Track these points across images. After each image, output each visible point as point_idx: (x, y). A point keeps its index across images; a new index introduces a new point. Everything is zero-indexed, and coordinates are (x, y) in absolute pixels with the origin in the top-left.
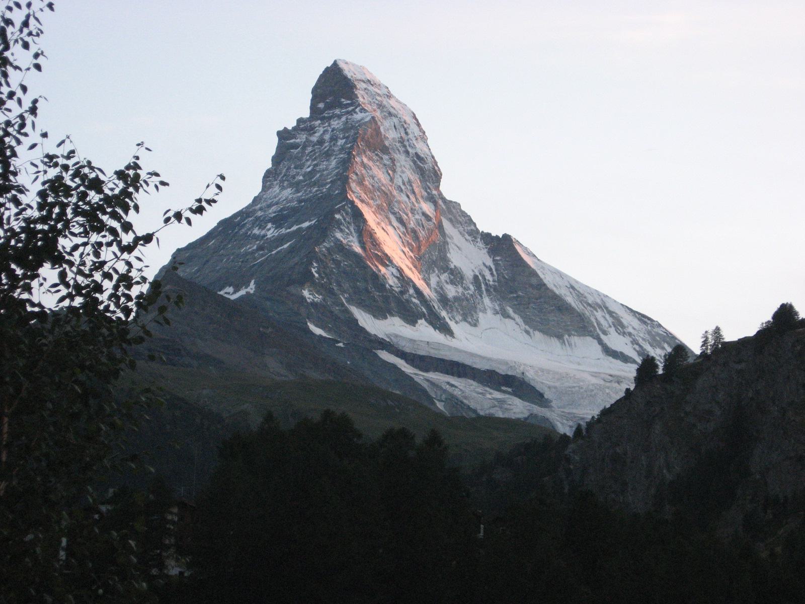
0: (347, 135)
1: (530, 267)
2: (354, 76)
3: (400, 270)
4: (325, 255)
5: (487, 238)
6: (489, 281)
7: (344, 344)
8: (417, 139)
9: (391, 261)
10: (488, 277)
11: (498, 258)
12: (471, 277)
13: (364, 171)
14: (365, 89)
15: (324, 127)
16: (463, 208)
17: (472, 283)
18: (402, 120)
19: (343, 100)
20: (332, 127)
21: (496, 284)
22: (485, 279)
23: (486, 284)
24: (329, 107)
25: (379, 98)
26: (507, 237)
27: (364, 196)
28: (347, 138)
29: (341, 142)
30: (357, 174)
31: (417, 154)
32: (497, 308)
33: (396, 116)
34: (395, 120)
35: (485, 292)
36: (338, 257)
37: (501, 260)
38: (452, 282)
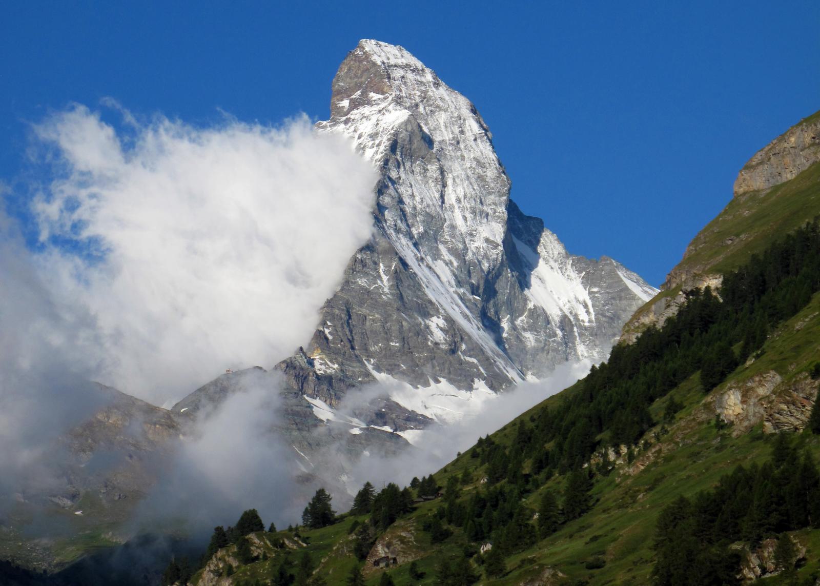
0: (377, 142)
2: (385, 61)
3: (449, 320)
4: (343, 310)
6: (583, 321)
7: (361, 429)
11: (595, 290)
12: (557, 319)
14: (403, 77)
15: (349, 133)
17: (559, 327)
19: (372, 94)
20: (359, 132)
21: (594, 325)
24: (355, 105)
25: (423, 88)
28: (379, 145)
29: (369, 153)
33: (446, 111)
35: (578, 338)
37: (598, 292)
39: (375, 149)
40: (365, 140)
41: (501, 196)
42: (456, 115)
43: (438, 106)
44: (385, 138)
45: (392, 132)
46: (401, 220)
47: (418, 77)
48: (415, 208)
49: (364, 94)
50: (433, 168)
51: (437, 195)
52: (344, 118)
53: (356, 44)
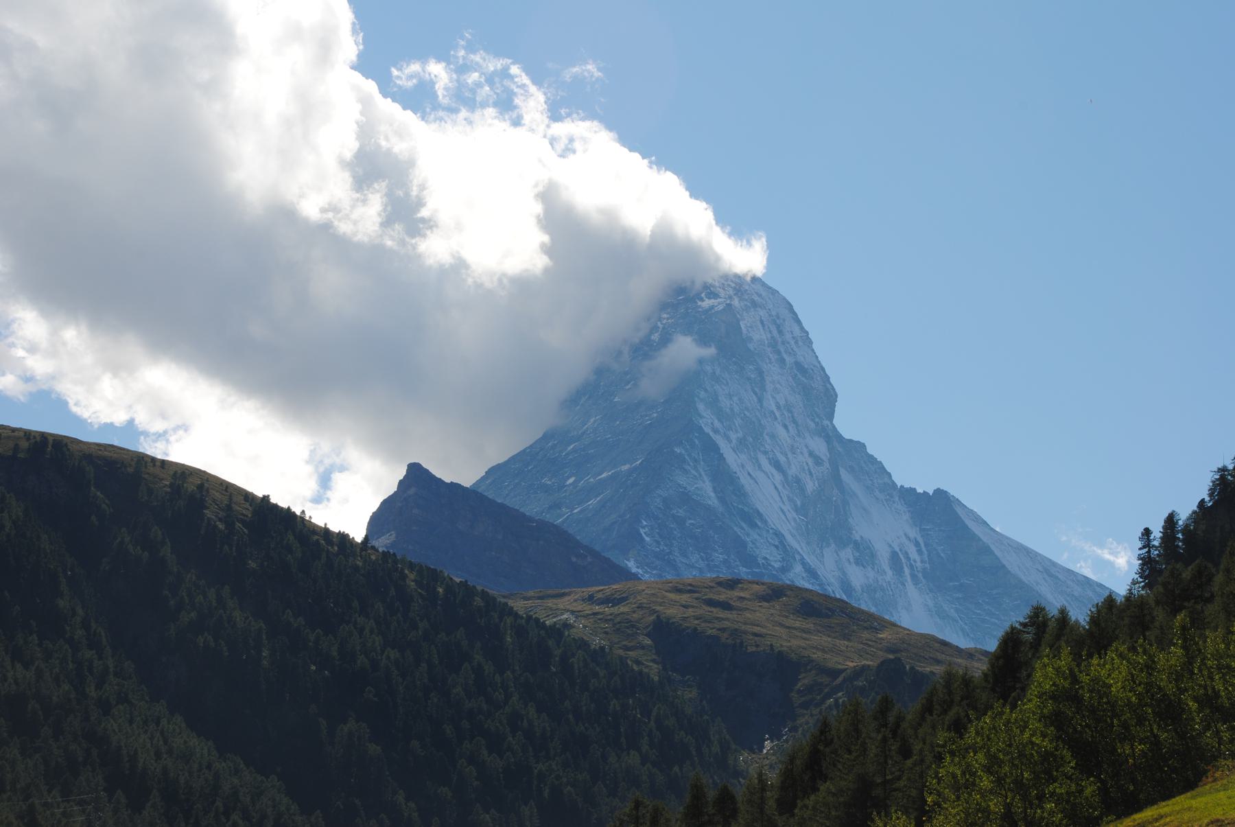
1: (980, 539)
3: (778, 534)
5: (909, 495)
8: (796, 343)
9: (765, 522)
10: (914, 555)
13: (717, 387)
16: (870, 451)
18: (774, 313)
22: (908, 558)
23: (911, 567)
26: (939, 492)
27: (717, 424)
30: (706, 390)
31: (798, 365)
32: (931, 603)
34: (762, 313)
36: (681, 513)
38: (858, 562)
48: (732, 410)
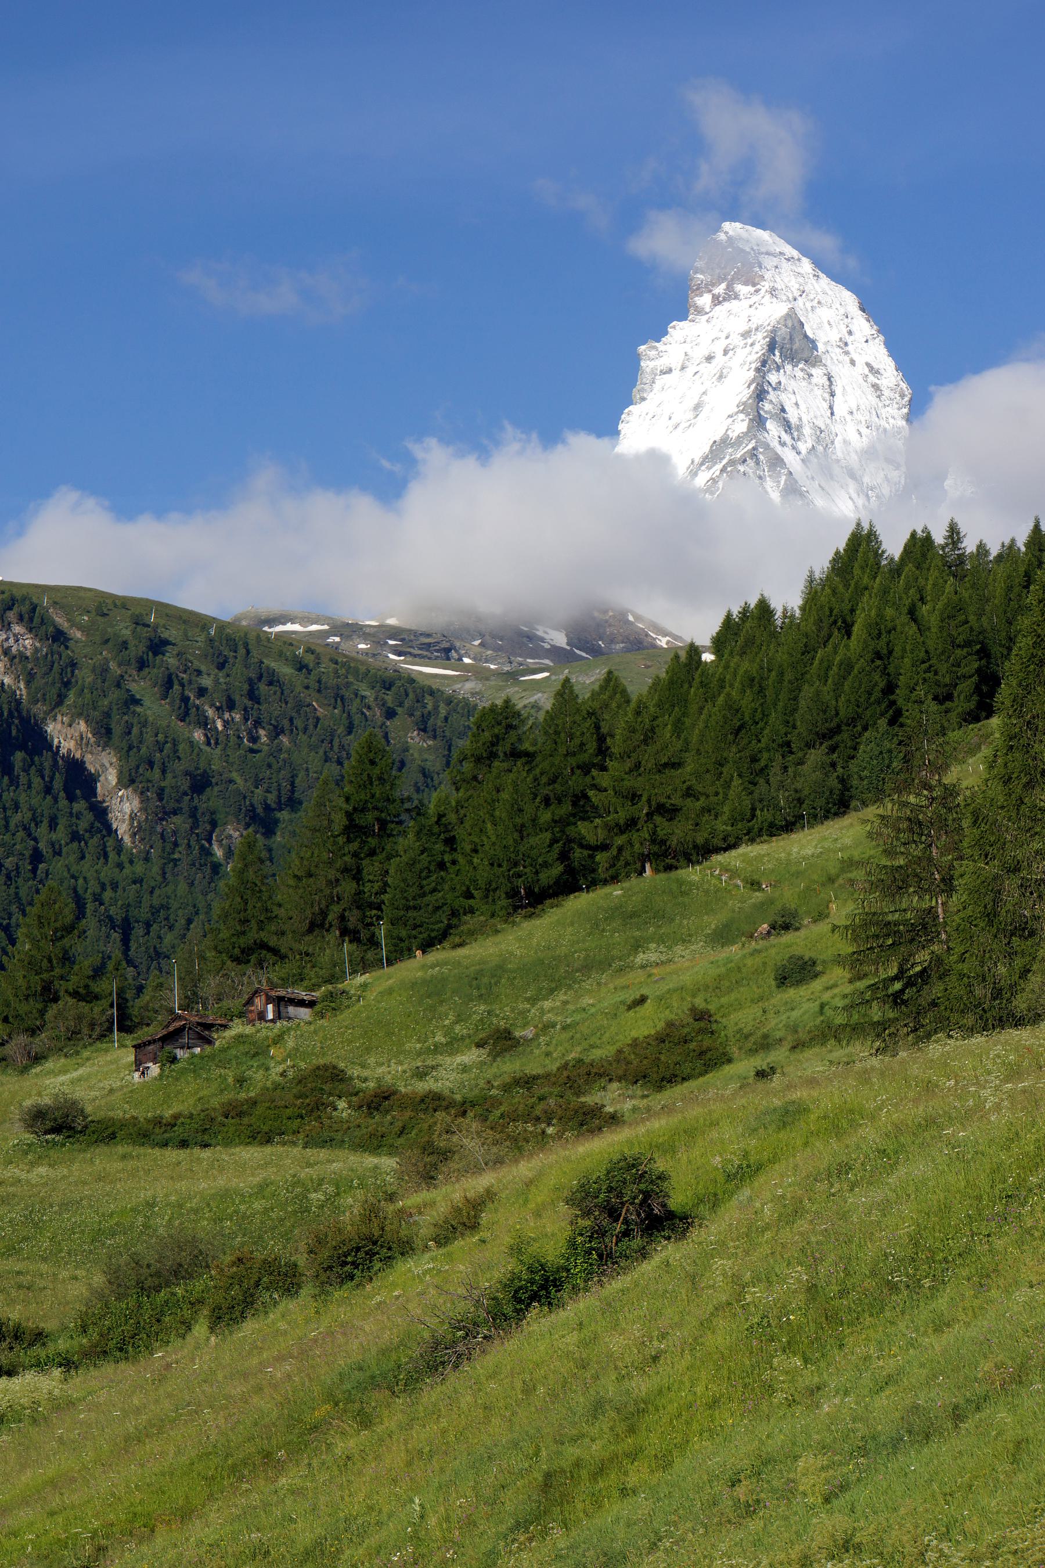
0: (749, 341)
14: (776, 267)
25: (801, 280)
27: (786, 438)
28: (752, 345)
31: (868, 364)
39: (749, 348)
40: (736, 340)
41: (899, 409)
42: (842, 311)
43: (819, 303)
44: (760, 336)
45: (769, 328)
46: (786, 431)
47: (794, 268)
48: (800, 419)
49: (729, 288)
50: (817, 372)
51: (826, 405)
52: (706, 317)
53: (718, 229)
